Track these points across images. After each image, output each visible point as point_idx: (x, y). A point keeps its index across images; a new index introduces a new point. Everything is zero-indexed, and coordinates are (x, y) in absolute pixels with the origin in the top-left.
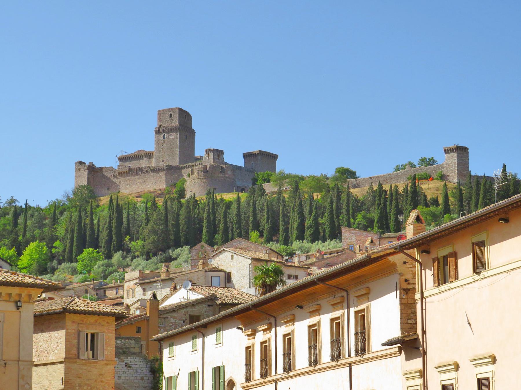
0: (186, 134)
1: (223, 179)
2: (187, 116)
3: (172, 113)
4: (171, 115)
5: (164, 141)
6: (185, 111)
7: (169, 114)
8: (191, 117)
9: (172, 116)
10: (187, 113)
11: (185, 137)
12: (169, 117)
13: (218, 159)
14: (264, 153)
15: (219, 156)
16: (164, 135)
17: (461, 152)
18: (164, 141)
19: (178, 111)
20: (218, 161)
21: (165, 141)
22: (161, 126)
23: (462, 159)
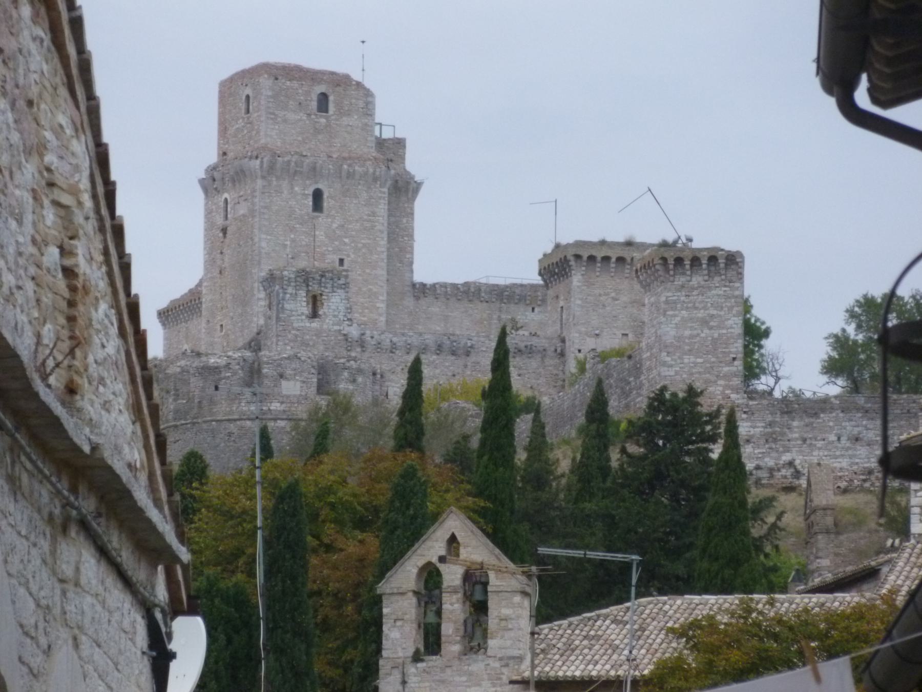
0: (320, 186)
1: (249, 423)
2: (331, 98)
3: (251, 95)
4: (248, 97)
5: (224, 231)
6: (323, 73)
7: (244, 98)
8: (368, 95)
9: (251, 107)
10: (342, 81)
11: (310, 202)
12: (243, 111)
13: (314, 315)
14: (599, 255)
15: (315, 302)
16: (226, 200)
17: (697, 280)
18: (224, 231)
19: (265, 82)
20: (315, 324)
21: (229, 232)
22: (225, 154)
23: (701, 314)
